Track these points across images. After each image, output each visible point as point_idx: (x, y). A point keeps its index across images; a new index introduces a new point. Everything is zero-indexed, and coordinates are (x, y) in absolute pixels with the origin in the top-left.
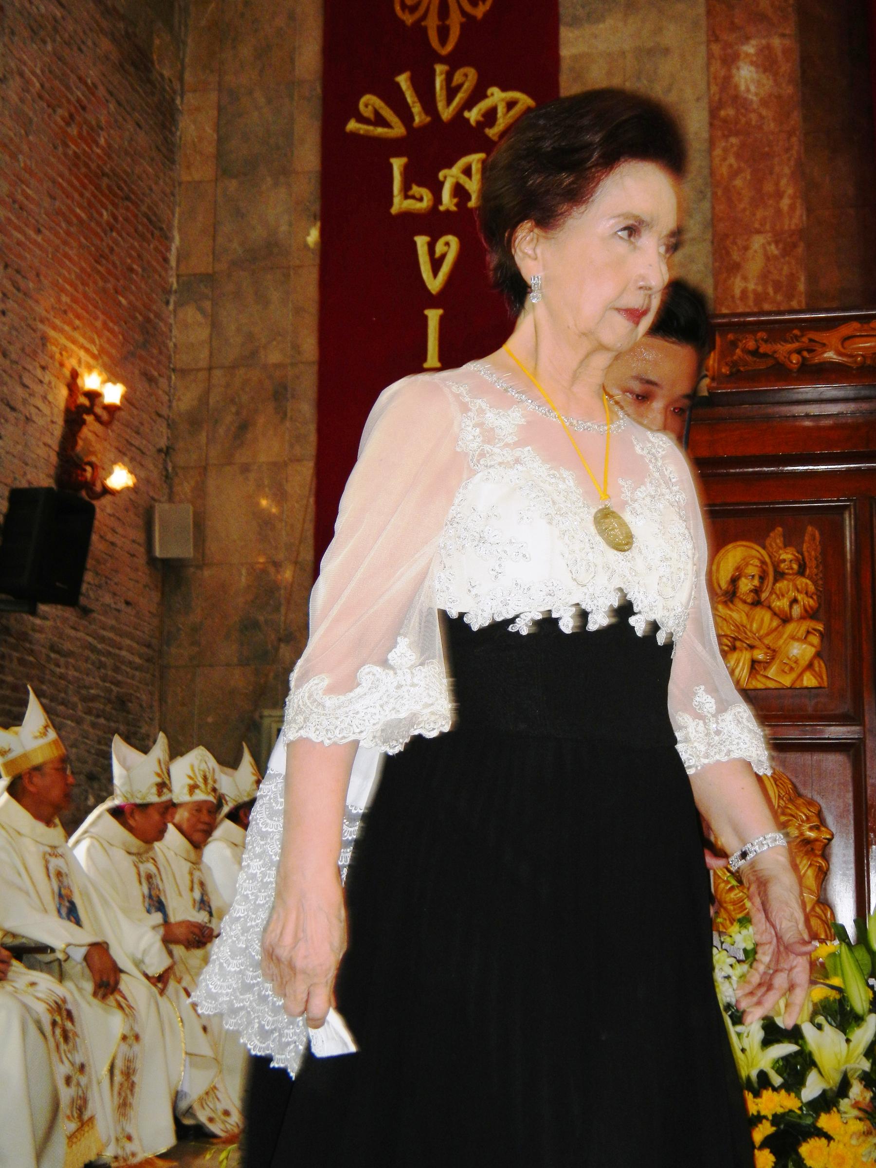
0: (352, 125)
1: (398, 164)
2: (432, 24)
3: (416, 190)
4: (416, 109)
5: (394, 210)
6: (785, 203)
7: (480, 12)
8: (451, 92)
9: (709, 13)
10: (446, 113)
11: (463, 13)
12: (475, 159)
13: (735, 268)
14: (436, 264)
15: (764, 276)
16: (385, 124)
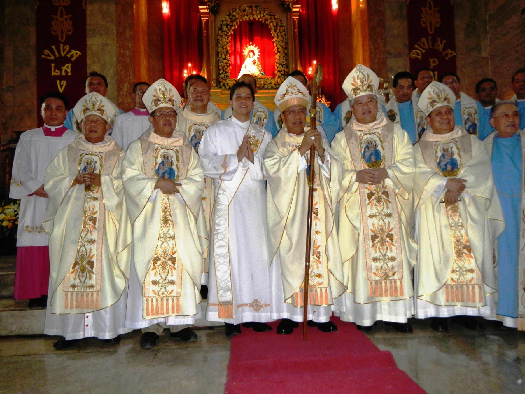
0: (43, 56)
1: (53, 65)
2: (60, 35)
3: (57, 71)
4: (57, 53)
5: (52, 75)
6: (131, 77)
7: (70, 33)
8: (64, 50)
9: (117, 38)
10: (63, 55)
11: (66, 33)
12: (69, 65)
13: (121, 89)
14: (61, 86)
15: (127, 91)
16: (50, 56)
